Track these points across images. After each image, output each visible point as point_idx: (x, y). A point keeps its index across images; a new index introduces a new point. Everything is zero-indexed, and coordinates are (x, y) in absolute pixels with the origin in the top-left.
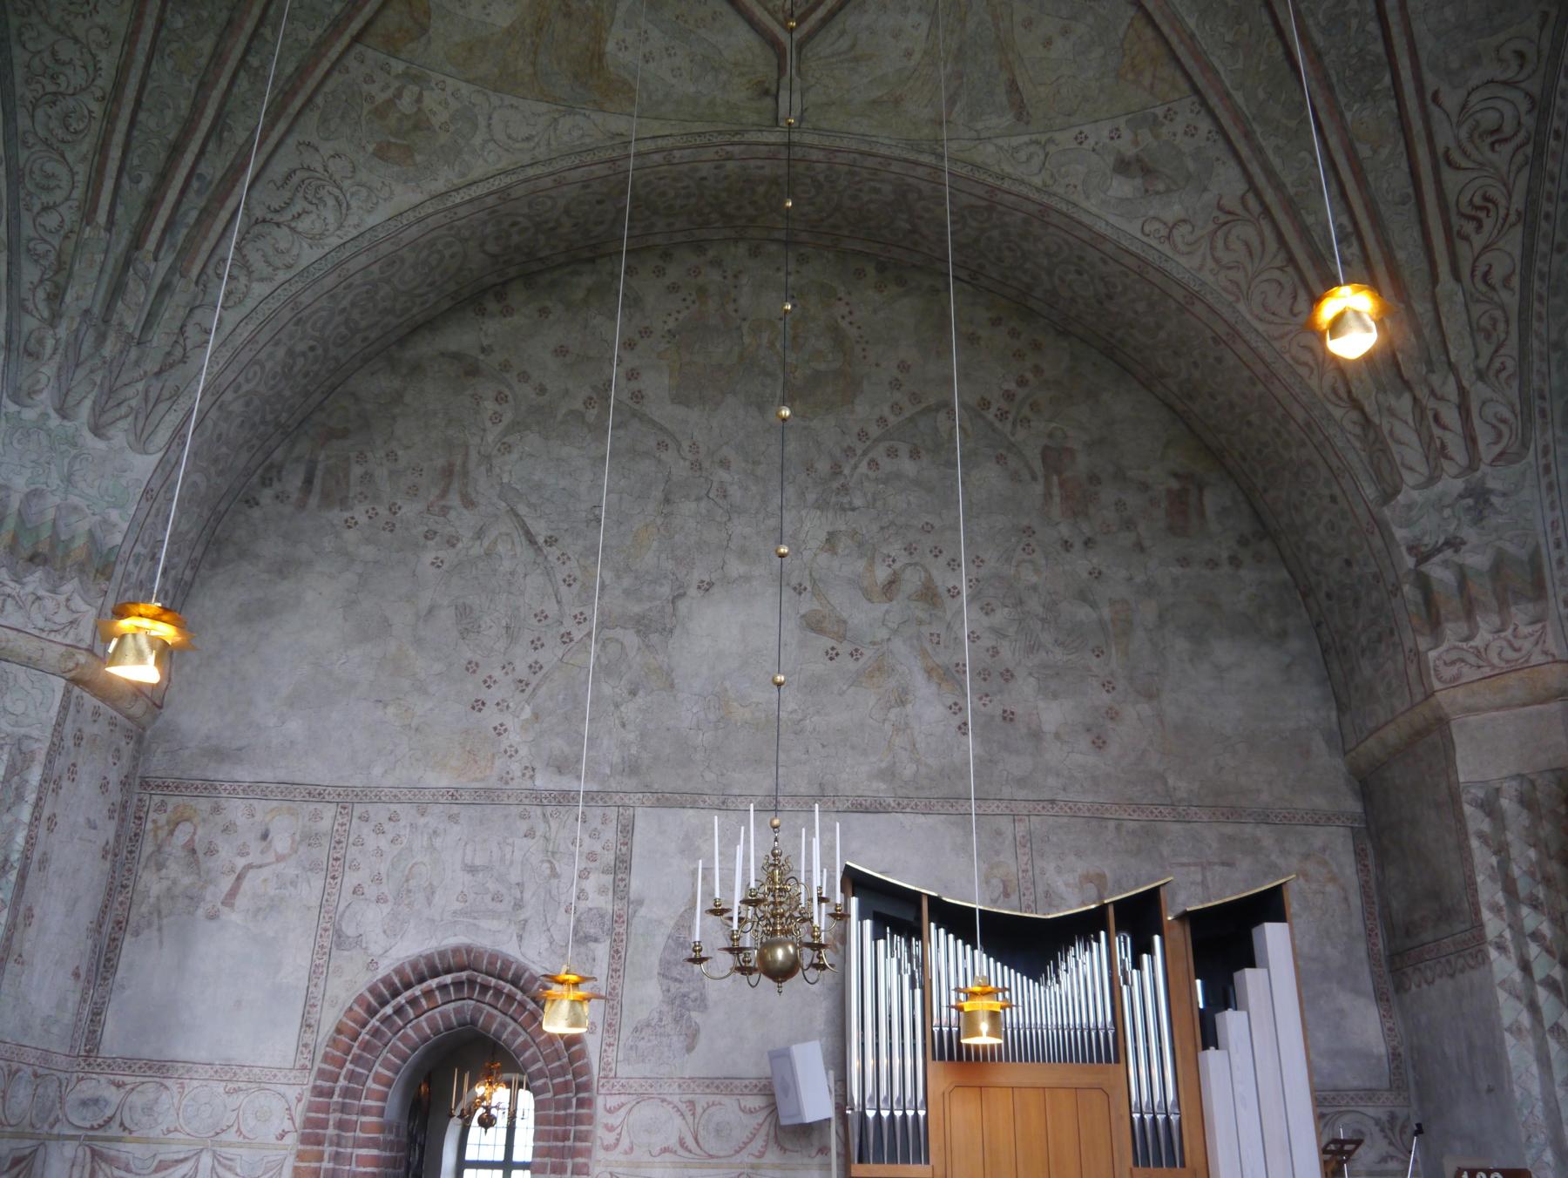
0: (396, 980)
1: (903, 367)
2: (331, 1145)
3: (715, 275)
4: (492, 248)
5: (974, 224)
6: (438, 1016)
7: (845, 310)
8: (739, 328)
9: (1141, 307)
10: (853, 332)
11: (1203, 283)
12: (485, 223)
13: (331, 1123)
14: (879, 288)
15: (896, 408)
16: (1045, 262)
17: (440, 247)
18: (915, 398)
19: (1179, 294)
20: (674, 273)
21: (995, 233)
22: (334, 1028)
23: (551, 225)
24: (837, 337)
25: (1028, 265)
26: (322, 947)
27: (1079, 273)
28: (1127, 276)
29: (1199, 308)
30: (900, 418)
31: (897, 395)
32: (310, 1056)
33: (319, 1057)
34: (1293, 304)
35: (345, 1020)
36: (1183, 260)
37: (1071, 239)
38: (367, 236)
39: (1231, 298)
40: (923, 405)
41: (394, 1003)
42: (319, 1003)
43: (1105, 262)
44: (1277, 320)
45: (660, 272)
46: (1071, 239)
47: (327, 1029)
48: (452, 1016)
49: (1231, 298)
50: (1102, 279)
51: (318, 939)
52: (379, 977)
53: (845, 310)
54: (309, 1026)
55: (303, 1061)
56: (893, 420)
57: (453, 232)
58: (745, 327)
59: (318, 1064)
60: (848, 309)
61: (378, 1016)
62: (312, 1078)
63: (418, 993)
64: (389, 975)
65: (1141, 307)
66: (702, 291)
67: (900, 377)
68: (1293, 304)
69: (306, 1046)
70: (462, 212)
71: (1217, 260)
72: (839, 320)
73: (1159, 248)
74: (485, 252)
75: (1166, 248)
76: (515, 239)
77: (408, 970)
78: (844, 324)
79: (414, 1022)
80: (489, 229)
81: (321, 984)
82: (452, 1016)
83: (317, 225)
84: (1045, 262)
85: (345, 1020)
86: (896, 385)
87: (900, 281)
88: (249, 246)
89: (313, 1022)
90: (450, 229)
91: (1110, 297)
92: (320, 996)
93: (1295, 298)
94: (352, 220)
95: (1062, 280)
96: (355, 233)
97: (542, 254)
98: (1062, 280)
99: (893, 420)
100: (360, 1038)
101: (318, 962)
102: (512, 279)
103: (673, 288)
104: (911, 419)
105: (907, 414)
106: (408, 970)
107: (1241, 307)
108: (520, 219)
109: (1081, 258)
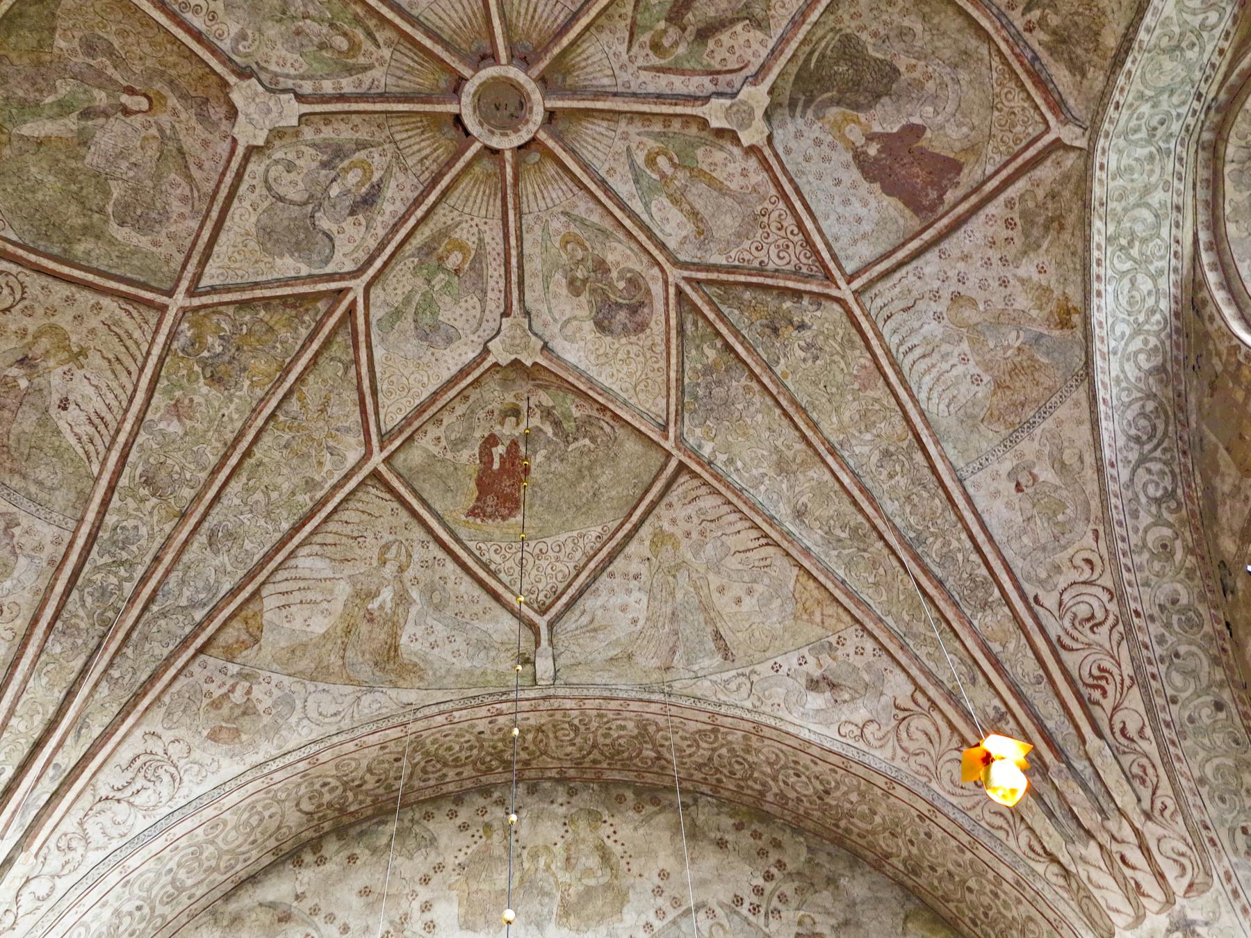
1: (663, 875)
3: (499, 812)
4: (307, 806)
7: (610, 831)
8: (519, 856)
9: (854, 797)
10: (617, 849)
11: (899, 770)
12: (299, 785)
14: (638, 809)
15: (660, 913)
16: (768, 770)
17: (260, 809)
18: (676, 902)
19: (880, 781)
20: (464, 814)
23: (357, 783)
24: (605, 856)
25: (756, 775)
27: (798, 776)
29: (900, 791)
30: (665, 922)
31: (660, 901)
36: (877, 753)
38: (194, 804)
39: (924, 780)
40: (683, 908)
43: (816, 763)
44: (966, 792)
45: (453, 815)
49: (924, 780)
53: (610, 831)
56: (657, 924)
57: (270, 795)
58: (525, 854)
60: (612, 829)
66: (488, 827)
67: (661, 884)
70: (278, 776)
72: (606, 839)
74: (300, 810)
76: (327, 798)
78: (609, 843)
80: (303, 790)
83: (152, 798)
84: (768, 770)
86: (658, 891)
87: (655, 801)
88: (90, 821)
90: (267, 793)
91: (827, 792)
94: (184, 791)
95: (785, 782)
96: (184, 802)
97: (352, 809)
99: (657, 924)
102: (327, 833)
103: (464, 827)
104: (674, 922)
105: (670, 917)
107: (934, 785)
108: (329, 780)
109: (796, 762)
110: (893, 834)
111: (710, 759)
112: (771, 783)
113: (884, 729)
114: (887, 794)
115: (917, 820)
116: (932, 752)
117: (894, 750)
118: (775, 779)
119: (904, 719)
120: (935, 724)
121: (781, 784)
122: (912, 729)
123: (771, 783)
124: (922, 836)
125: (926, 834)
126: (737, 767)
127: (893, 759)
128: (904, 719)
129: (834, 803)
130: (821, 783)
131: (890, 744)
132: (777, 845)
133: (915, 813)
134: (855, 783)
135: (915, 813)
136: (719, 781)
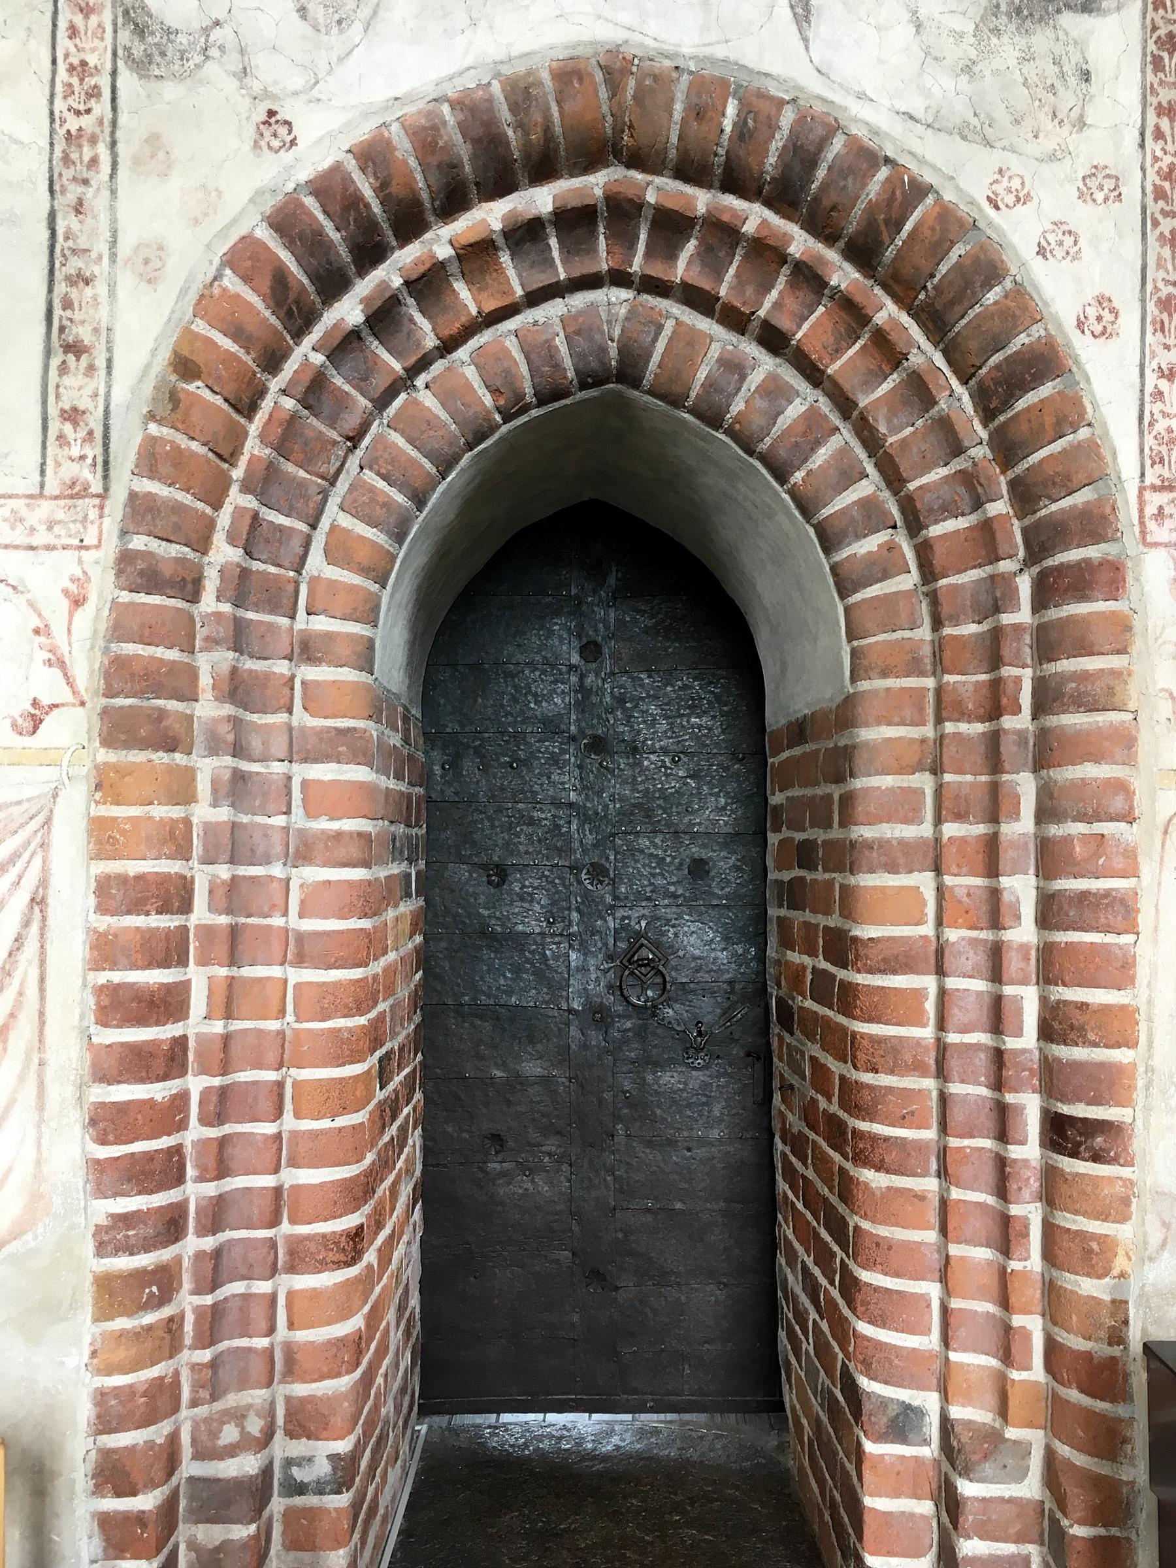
0: (366, 188)
2: (213, 750)
6: (512, 344)
13: (205, 681)
22: (165, 354)
26: (81, 69)
32: (94, 451)
33: (126, 454)
35: (201, 327)
41: (364, 287)
42: (101, 270)
47: (140, 357)
48: (560, 342)
51: (63, 42)
52: (304, 175)
54: (75, 349)
55: (70, 470)
59: (124, 481)
61: (317, 333)
62: (111, 525)
63: (444, 252)
64: (337, 168)
69: (73, 415)
77: (403, 147)
79: (438, 366)
81: (97, 199)
82: (560, 342)
85: (201, 327)
89: (84, 333)
92: (103, 247)
100: (267, 405)
101: (73, 124)
106: (403, 147)
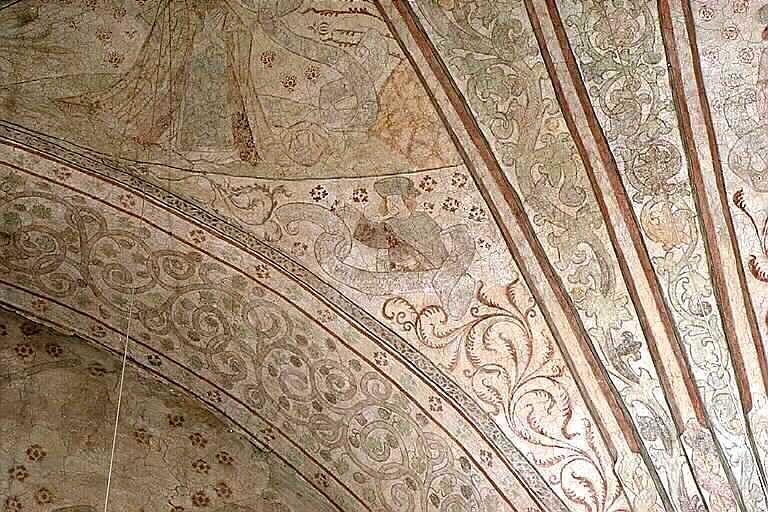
5: (166, 278)
9: (371, 414)
21: (194, 297)
27: (298, 364)
28: (358, 367)
34: (566, 423)
37: (292, 312)
43: (332, 347)
46: (292, 312)
50: (325, 371)
65: (371, 414)
68: (566, 423)
71: (473, 360)
73: (403, 334)
75: (411, 337)
91: (331, 399)
93: (569, 415)
95: (272, 371)
98: (272, 371)
107: (500, 419)
110: (410, 482)
111: (167, 305)
112: (250, 366)
113: (452, 324)
114: (425, 416)
115: (458, 465)
116: (513, 375)
117: (458, 357)
118: (257, 363)
119: (486, 317)
120: (529, 335)
121: (265, 371)
122: (493, 334)
123: (250, 366)
124: (457, 491)
125: (463, 489)
126: (205, 327)
127: (451, 369)
128: (486, 317)
129: (335, 417)
130: (328, 381)
131: (454, 347)
132: (226, 461)
133: (458, 453)
134: (382, 391)
135: (458, 453)
136: (168, 345)
